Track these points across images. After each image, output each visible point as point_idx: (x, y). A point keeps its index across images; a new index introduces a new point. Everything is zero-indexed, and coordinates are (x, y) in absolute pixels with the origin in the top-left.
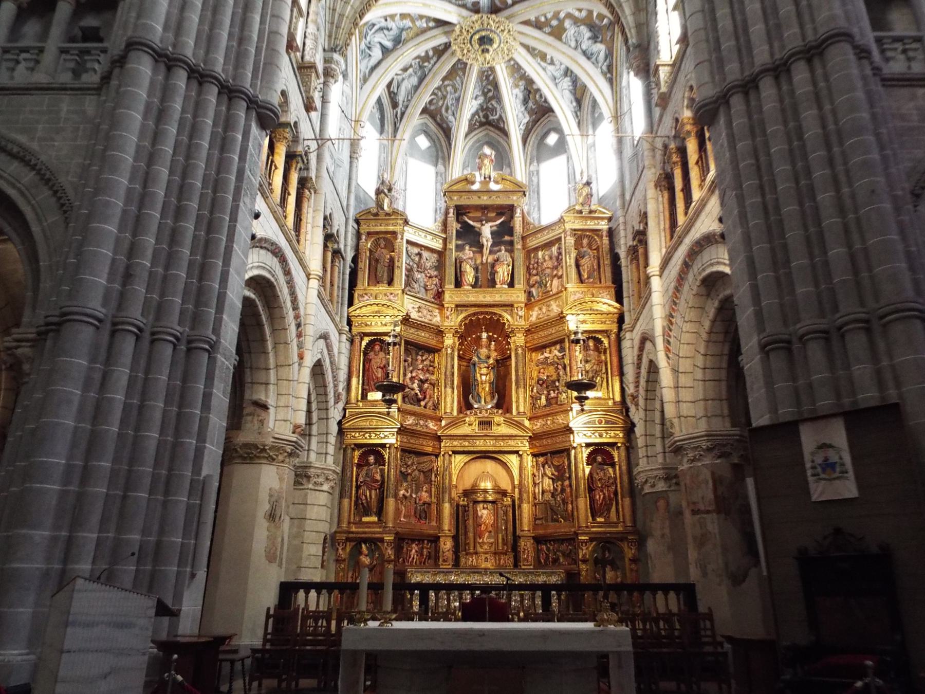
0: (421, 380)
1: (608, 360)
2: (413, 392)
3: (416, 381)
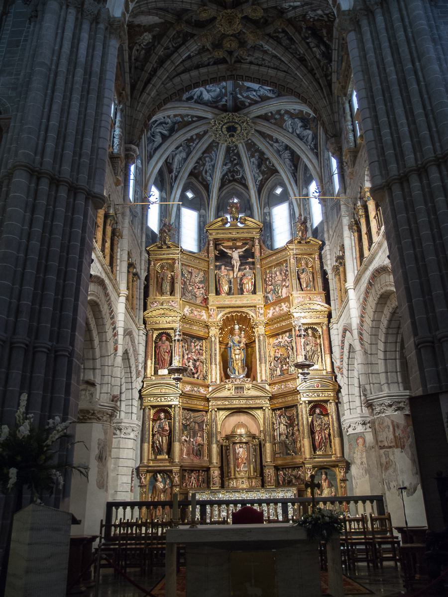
0: (194, 360)
1: (322, 343)
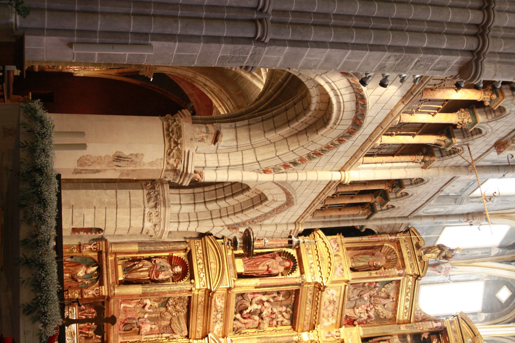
0: (261, 313)
2: (248, 304)
3: (259, 307)
